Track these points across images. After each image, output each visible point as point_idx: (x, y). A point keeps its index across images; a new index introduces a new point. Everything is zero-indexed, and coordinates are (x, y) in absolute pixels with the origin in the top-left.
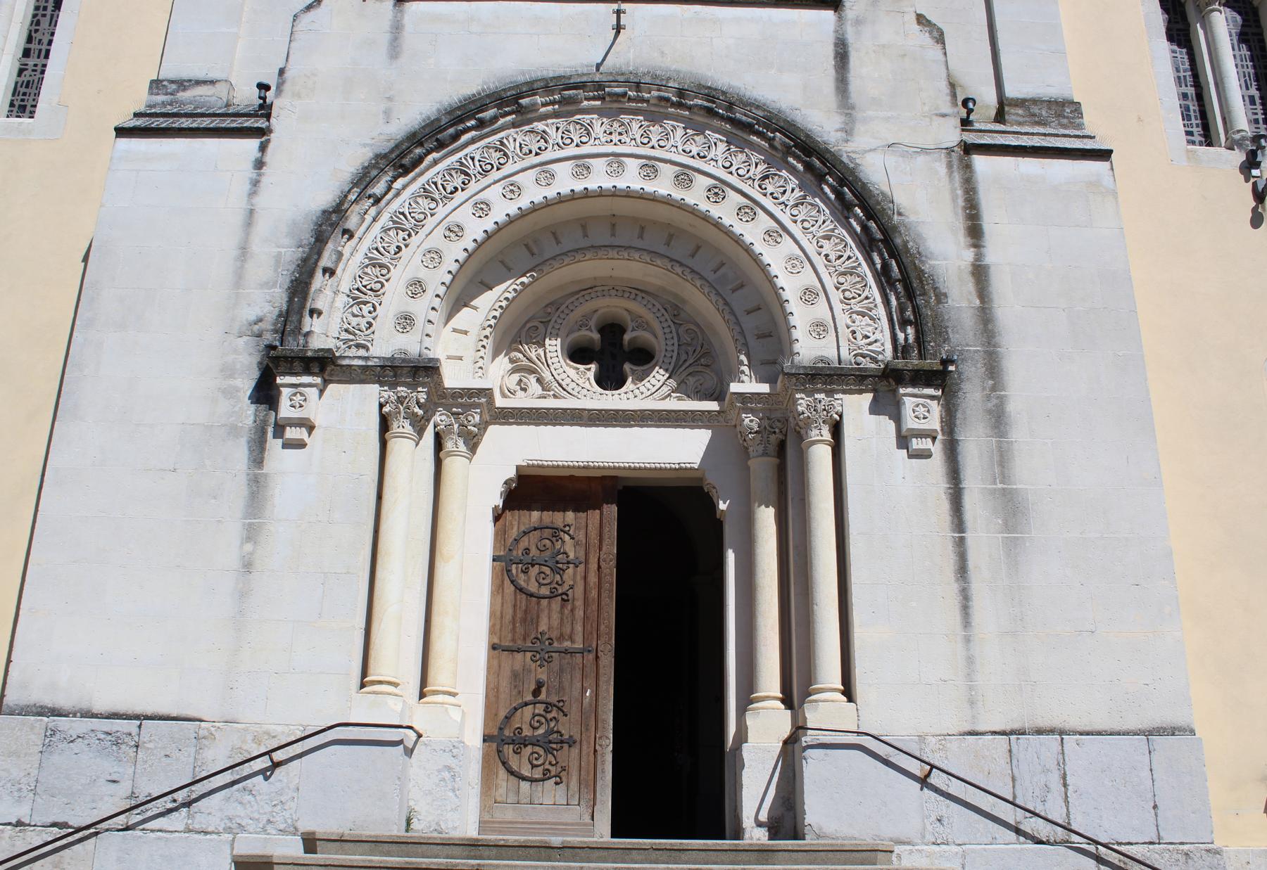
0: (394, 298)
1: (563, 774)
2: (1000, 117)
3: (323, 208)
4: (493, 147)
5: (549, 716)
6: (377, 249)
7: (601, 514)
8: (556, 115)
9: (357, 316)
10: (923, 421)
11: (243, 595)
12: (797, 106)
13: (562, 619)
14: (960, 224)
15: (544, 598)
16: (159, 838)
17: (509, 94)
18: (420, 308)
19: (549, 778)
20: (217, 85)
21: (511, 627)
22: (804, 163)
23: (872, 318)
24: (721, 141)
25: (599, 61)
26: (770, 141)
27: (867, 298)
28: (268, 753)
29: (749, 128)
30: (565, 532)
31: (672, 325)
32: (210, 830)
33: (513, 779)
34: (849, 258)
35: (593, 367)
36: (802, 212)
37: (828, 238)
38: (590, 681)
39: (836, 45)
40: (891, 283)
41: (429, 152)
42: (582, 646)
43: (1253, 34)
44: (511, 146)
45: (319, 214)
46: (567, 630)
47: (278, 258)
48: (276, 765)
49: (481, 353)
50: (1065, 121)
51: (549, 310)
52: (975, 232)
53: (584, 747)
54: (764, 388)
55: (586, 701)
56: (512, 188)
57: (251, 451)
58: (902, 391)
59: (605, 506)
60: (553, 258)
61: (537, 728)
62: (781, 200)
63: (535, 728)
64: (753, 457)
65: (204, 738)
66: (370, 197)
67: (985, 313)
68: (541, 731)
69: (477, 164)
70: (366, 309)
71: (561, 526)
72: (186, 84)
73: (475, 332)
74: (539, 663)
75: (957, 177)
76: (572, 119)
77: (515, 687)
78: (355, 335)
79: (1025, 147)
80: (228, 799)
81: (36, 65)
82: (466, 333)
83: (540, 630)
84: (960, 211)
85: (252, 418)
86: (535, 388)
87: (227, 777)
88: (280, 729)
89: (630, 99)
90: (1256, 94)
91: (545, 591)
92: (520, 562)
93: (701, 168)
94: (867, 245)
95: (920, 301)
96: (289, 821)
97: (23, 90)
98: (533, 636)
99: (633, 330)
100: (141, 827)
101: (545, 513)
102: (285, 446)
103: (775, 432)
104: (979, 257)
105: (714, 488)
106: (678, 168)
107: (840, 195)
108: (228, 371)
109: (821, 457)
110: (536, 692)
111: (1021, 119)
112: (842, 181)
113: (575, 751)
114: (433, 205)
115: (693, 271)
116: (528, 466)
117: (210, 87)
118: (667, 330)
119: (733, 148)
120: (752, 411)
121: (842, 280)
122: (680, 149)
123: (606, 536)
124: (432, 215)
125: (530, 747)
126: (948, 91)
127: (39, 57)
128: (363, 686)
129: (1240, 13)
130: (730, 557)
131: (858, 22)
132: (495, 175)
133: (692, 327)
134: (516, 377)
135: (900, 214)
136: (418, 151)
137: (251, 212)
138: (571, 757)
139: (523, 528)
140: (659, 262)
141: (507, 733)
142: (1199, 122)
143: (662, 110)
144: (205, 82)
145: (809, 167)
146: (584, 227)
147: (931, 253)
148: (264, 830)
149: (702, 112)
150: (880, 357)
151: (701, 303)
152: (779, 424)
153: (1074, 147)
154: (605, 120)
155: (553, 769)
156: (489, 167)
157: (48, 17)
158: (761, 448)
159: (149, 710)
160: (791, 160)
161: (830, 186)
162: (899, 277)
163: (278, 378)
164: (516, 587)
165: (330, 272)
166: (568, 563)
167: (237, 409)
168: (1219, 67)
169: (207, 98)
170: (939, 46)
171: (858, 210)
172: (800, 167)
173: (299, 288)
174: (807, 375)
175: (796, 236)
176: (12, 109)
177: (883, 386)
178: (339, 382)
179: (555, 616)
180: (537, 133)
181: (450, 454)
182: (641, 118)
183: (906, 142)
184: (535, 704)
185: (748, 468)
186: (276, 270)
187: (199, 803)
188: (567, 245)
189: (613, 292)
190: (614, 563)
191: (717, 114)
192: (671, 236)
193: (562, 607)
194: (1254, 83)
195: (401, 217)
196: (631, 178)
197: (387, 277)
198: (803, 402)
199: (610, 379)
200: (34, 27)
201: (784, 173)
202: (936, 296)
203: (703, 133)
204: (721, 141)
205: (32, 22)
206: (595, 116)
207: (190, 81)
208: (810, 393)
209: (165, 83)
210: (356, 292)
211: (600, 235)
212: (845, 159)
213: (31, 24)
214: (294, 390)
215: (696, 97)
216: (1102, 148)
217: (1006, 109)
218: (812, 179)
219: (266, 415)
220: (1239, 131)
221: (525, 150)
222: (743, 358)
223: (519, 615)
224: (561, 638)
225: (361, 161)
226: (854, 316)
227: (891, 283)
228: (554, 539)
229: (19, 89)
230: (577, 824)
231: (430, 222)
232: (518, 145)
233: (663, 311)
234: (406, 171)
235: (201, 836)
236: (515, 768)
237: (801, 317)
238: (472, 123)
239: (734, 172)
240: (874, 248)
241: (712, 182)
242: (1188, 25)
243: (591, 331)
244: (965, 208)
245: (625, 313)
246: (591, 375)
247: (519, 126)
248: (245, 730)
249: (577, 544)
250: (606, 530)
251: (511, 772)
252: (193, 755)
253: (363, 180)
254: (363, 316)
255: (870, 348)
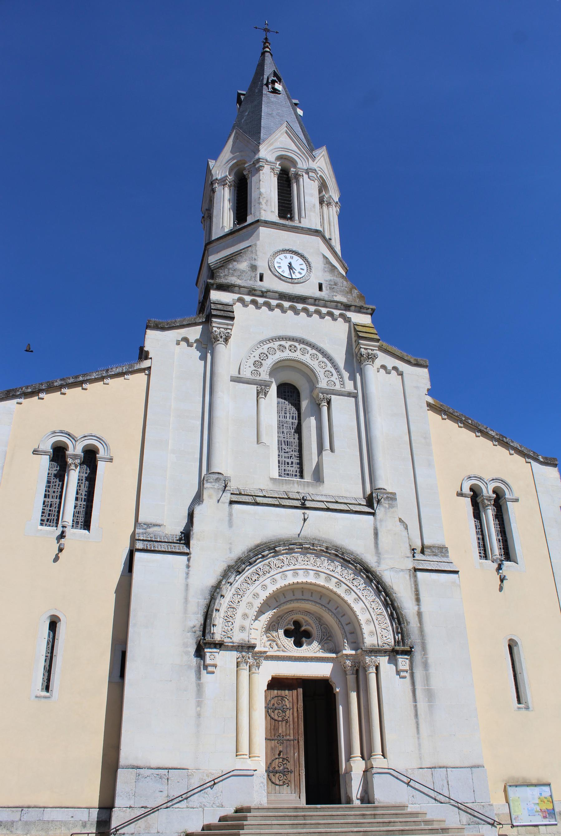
0: (238, 621)
1: (289, 783)
2: (422, 552)
3: (212, 585)
4: (267, 565)
5: (284, 763)
6: (231, 601)
7: (297, 692)
8: (287, 553)
9: (227, 626)
10: (404, 666)
11: (198, 725)
12: (363, 553)
13: (286, 729)
14: (413, 597)
15: (280, 721)
16: (179, 811)
17: (272, 546)
18: (247, 623)
19: (285, 784)
20: (161, 527)
21: (270, 731)
22: (391, 611)
23: (387, 630)
24: (339, 565)
25: (299, 533)
26: (356, 567)
27: (386, 623)
28: (214, 780)
29: (349, 562)
30: (285, 698)
31: (319, 625)
32: (195, 807)
33: (273, 785)
34: (380, 609)
35: (293, 639)
36: (365, 593)
37: (373, 602)
38: (296, 750)
39: (374, 529)
40: (393, 618)
41: (247, 566)
42: (293, 738)
43: (500, 515)
44: (272, 564)
45: (210, 587)
46: (288, 732)
47: (198, 603)
48: (215, 784)
49: (262, 637)
50: (443, 554)
51: (279, 619)
52: (418, 600)
53: (296, 773)
54: (353, 652)
55: (295, 757)
56: (273, 580)
57: (196, 675)
58: (398, 657)
59: (298, 689)
60: (284, 603)
61: (280, 767)
62: (358, 588)
63: (279, 767)
64: (349, 675)
65: (190, 775)
66: (229, 583)
67: (421, 628)
68: (281, 768)
69: (261, 570)
70: (230, 623)
71: (284, 696)
72: (150, 525)
73: (260, 629)
74: (279, 744)
75: (412, 580)
76: (292, 555)
77: (272, 752)
78: (227, 633)
79: (433, 570)
80: (199, 796)
81: (81, 505)
82: (257, 630)
83: (279, 732)
84: (413, 592)
85: (195, 662)
86: (276, 648)
87: (199, 789)
88: (214, 772)
89: (311, 549)
90: (501, 538)
91: (280, 719)
92: (272, 708)
93: (334, 575)
94: (386, 605)
95: (403, 626)
96: (220, 803)
97: (77, 515)
98: (277, 735)
99: (305, 626)
100: (172, 807)
101: (279, 691)
102: (207, 673)
103: (356, 667)
104: (419, 609)
105: (334, 683)
106: (326, 575)
107: (377, 588)
108: (185, 645)
109: (373, 677)
110: (279, 754)
111: (429, 554)
112: (378, 583)
113: (293, 774)
114: (248, 586)
115: (329, 609)
116: (275, 675)
117: (159, 527)
118: (318, 627)
119: (343, 568)
120: (349, 660)
121: (378, 617)
122: (327, 568)
123: (299, 699)
124: (249, 589)
125: (278, 774)
126: (409, 548)
127: (81, 501)
128: (237, 756)
129: (496, 508)
130: (341, 709)
131: (381, 521)
132: (268, 575)
133: (326, 626)
134: (269, 642)
135: (395, 593)
136: (243, 566)
137: (187, 585)
138: (291, 777)
139: (272, 696)
140: (317, 605)
141: (271, 769)
142: (483, 548)
143: (321, 553)
144: (157, 525)
145: (368, 577)
146: (293, 592)
147: (405, 608)
148: (212, 806)
149: (334, 555)
150: (390, 644)
151: (329, 619)
152: (357, 664)
153: (448, 570)
154: (302, 556)
155: (286, 781)
156: (266, 572)
157: (84, 484)
158: (351, 672)
159: (170, 766)
160: (362, 573)
161: (374, 584)
162: (396, 617)
163: (205, 649)
164: (271, 718)
165: (217, 610)
166: (287, 709)
167: (190, 659)
168: (490, 530)
169: (159, 532)
170: (406, 531)
171: (383, 593)
172: (365, 576)
173: (207, 616)
174: (369, 651)
175: (364, 601)
176: (73, 523)
177: (392, 654)
178: (223, 650)
179: (284, 727)
180: (281, 560)
181: (253, 673)
182: (314, 556)
183: (396, 567)
184: (279, 758)
185: (347, 678)
186: (198, 608)
187: (190, 798)
188: (288, 598)
189: (299, 613)
190: (302, 709)
191: (339, 556)
192: (321, 596)
193: (286, 724)
194: (500, 534)
195: (238, 589)
196: (311, 579)
197: (235, 612)
198: (368, 659)
199: (298, 644)
200: (78, 488)
201: (359, 578)
202: (406, 622)
203: (334, 562)
204: (339, 565)
205: (78, 485)
206: (299, 554)
207: (151, 524)
208: (370, 656)
209: (142, 524)
210: (226, 617)
211: (298, 595)
212: (378, 573)
213: (77, 487)
214: (210, 654)
215: (332, 550)
216: (456, 570)
217: (425, 549)
218: (368, 581)
219: (200, 662)
220: (496, 555)
221: (277, 566)
222: (345, 641)
223: (272, 727)
224: (286, 735)
225: (223, 568)
226: (382, 630)
227: (393, 618)
228: (282, 700)
229: (75, 514)
230: (295, 800)
231: (248, 592)
232: (274, 564)
233: (316, 620)
234: (240, 573)
235: (192, 809)
236: (274, 781)
237: (366, 629)
238: (260, 556)
239: (344, 577)
240: (388, 606)
241: (337, 580)
242: (480, 511)
243: (292, 626)
244: (415, 591)
245: (302, 619)
246: (292, 642)
247: (274, 557)
248: (203, 772)
249: (289, 702)
250: (299, 697)
251: (273, 783)
252: (187, 782)
253: (225, 575)
254: (229, 627)
255: (387, 641)
